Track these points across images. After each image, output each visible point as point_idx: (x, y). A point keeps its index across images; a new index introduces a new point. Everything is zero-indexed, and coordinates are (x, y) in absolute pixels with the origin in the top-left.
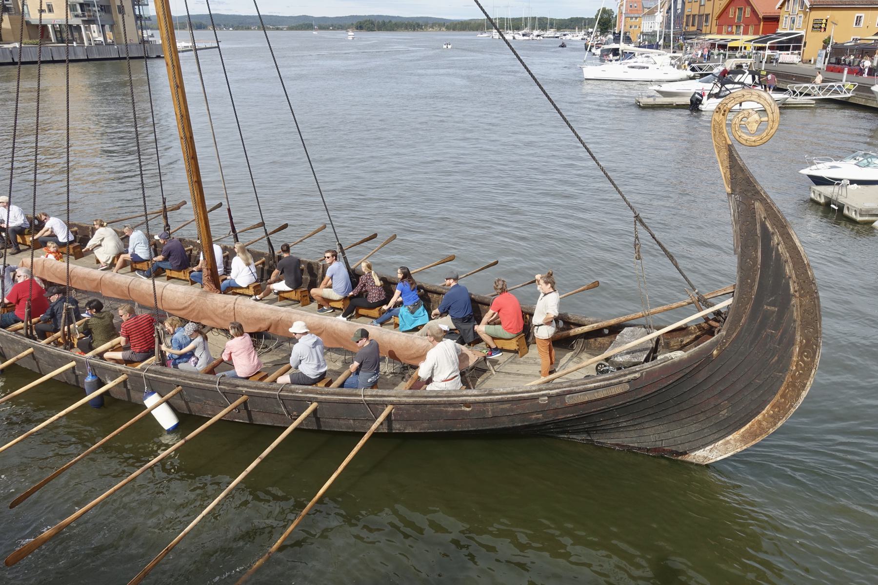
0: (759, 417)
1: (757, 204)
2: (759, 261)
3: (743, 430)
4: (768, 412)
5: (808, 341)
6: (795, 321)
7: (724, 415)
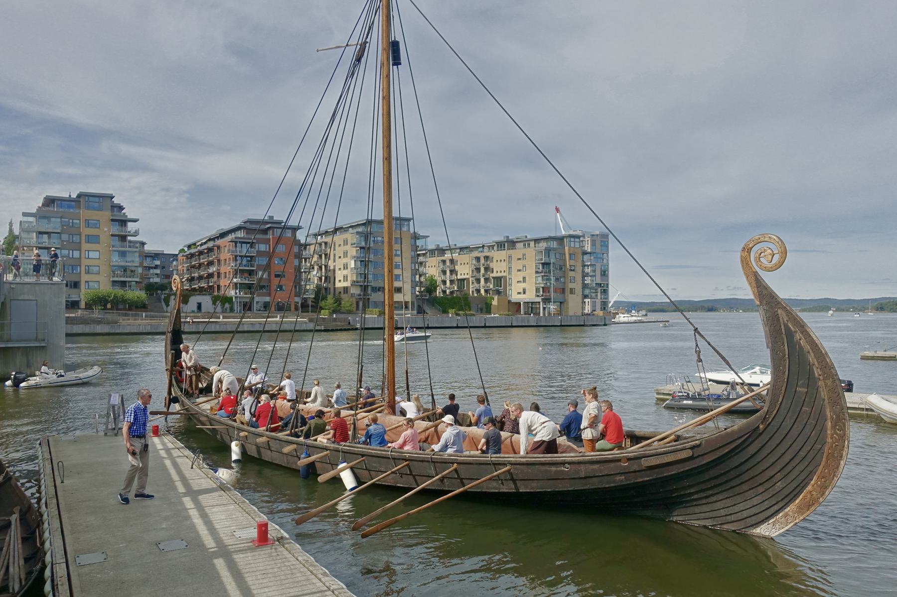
0: (809, 488)
2: (787, 353)
4: (816, 483)
5: (838, 416)
6: (824, 400)
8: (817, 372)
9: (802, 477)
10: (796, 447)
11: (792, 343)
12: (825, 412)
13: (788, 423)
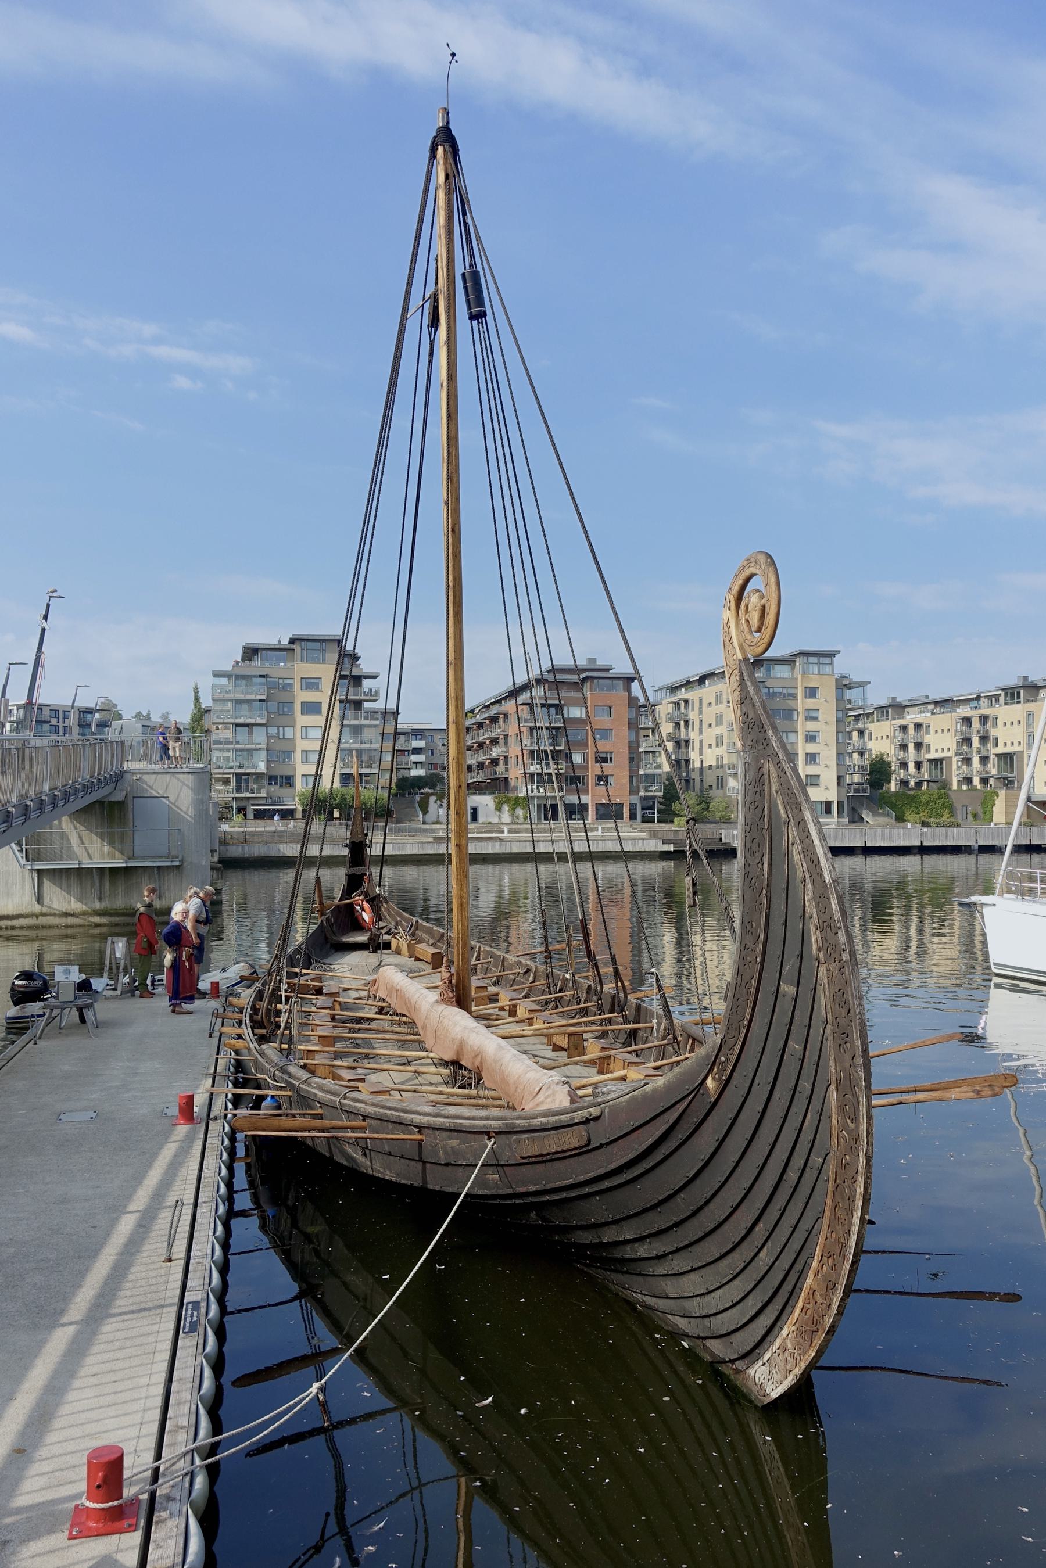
0: (810, 1280)
3: (797, 1312)
7: (764, 1261)
8: (815, 937)
9: (795, 1245)
12: (827, 1061)
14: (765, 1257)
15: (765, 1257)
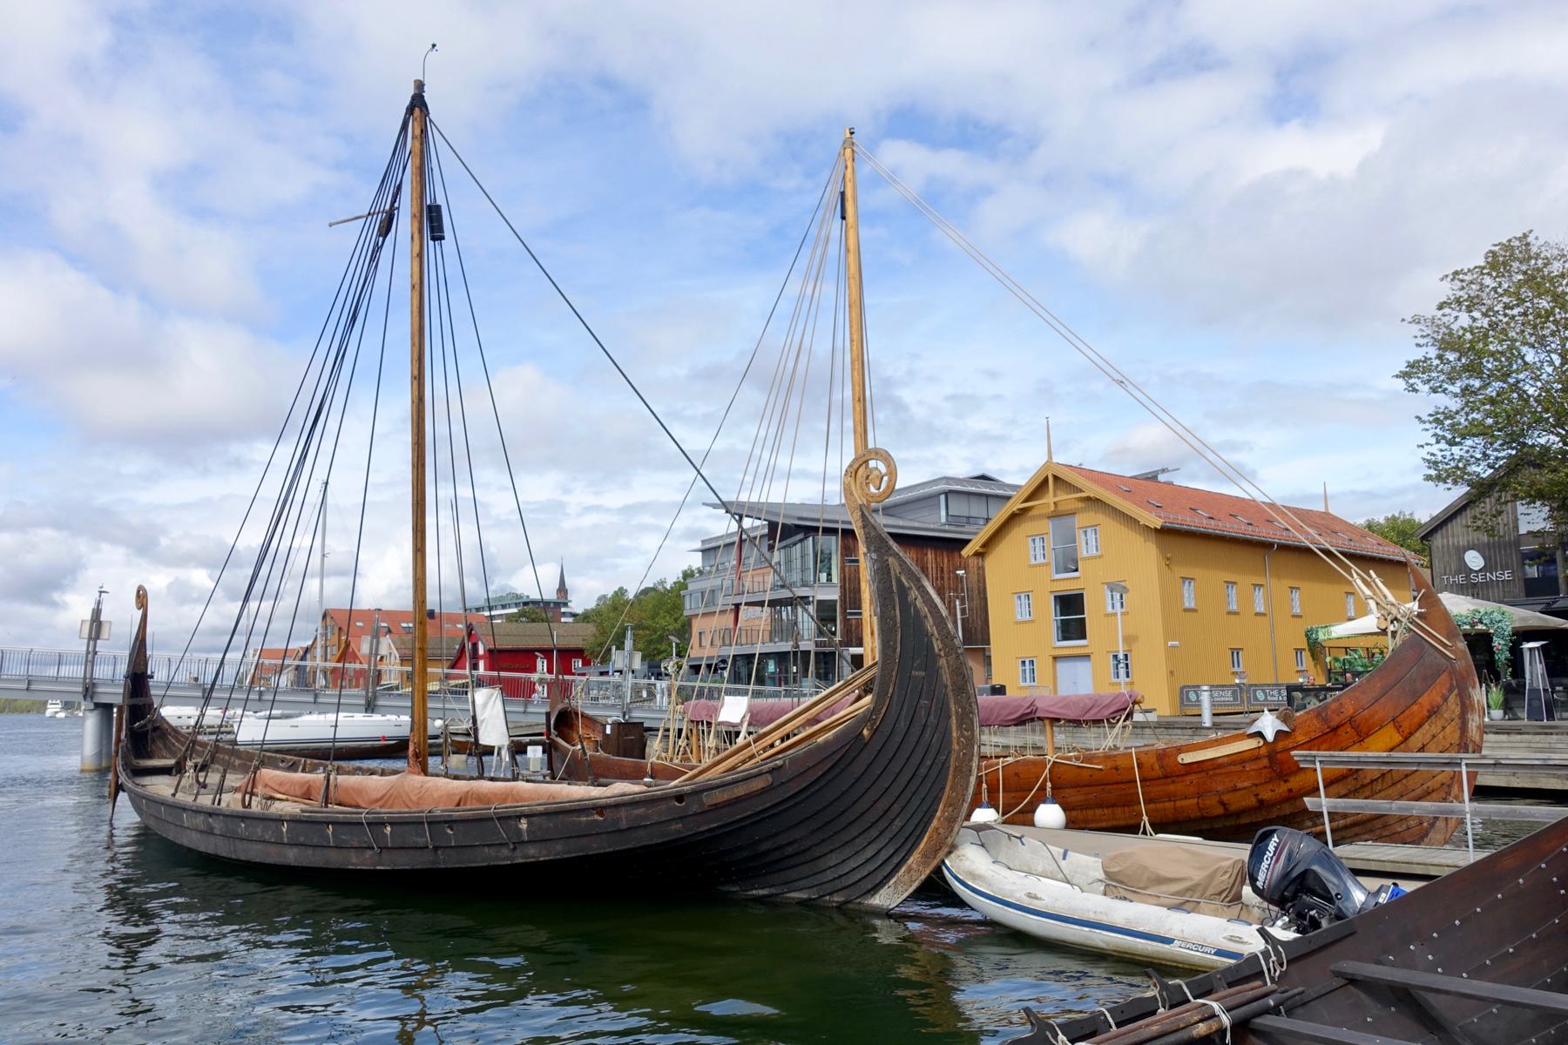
0: (935, 823)
1: (891, 560)
5: (964, 709)
8: (937, 645)
10: (915, 760)
11: (905, 605)
13: (903, 725)
14: (898, 823)
15: (898, 823)
